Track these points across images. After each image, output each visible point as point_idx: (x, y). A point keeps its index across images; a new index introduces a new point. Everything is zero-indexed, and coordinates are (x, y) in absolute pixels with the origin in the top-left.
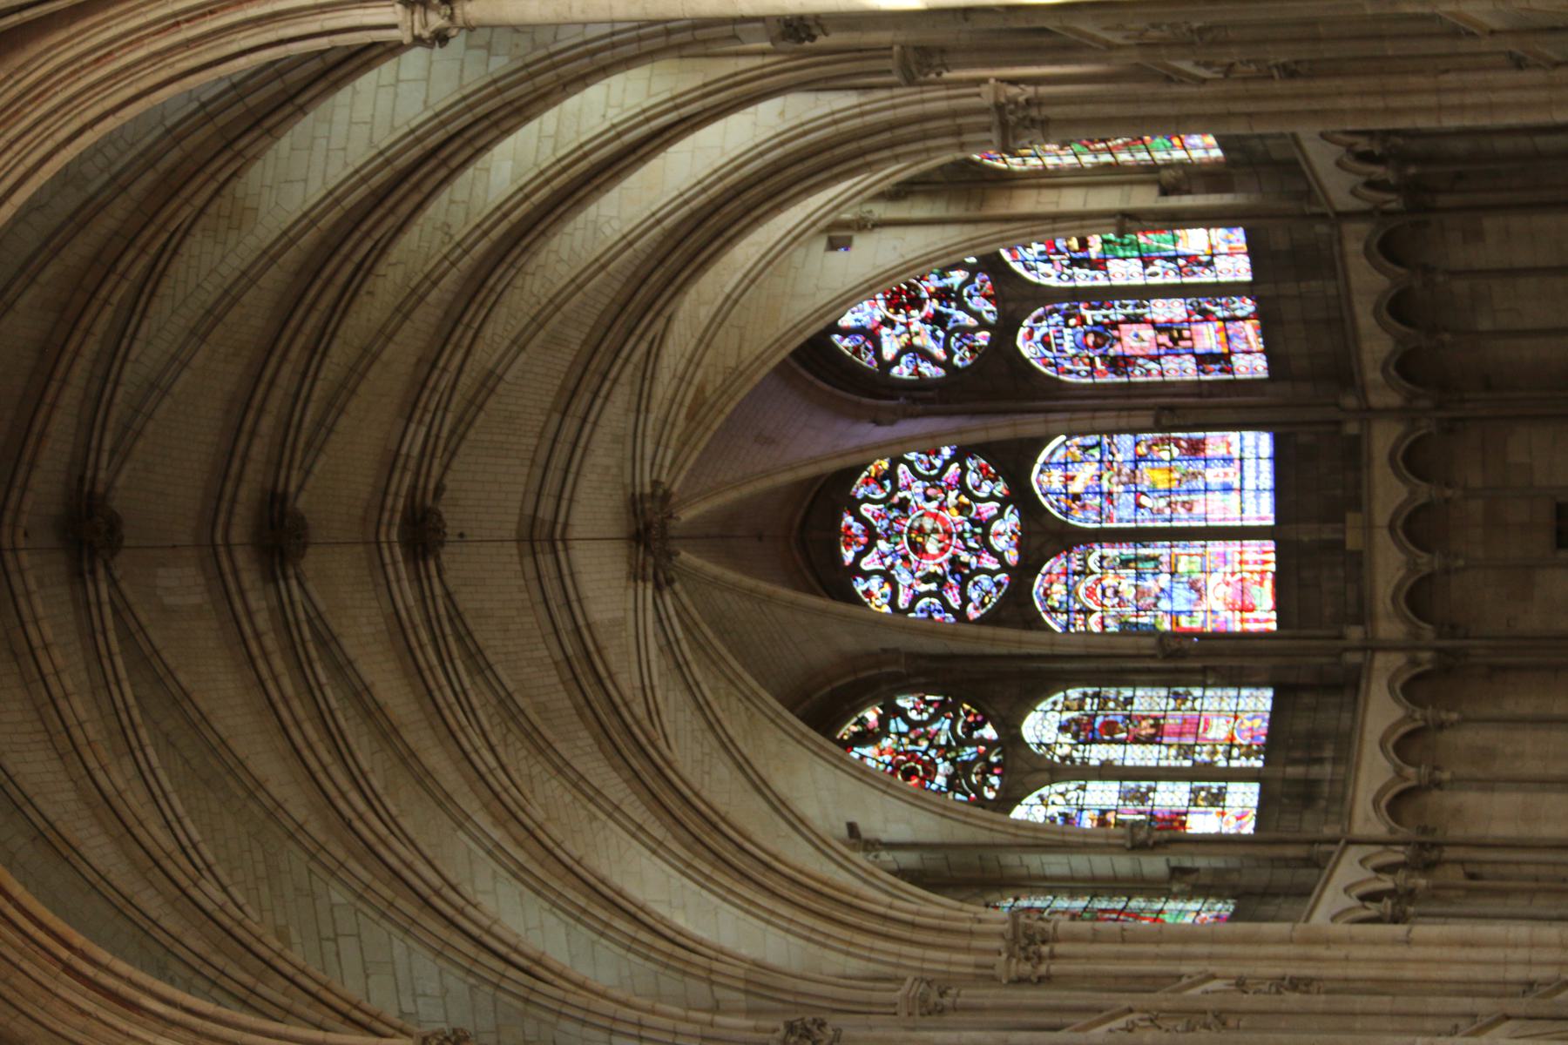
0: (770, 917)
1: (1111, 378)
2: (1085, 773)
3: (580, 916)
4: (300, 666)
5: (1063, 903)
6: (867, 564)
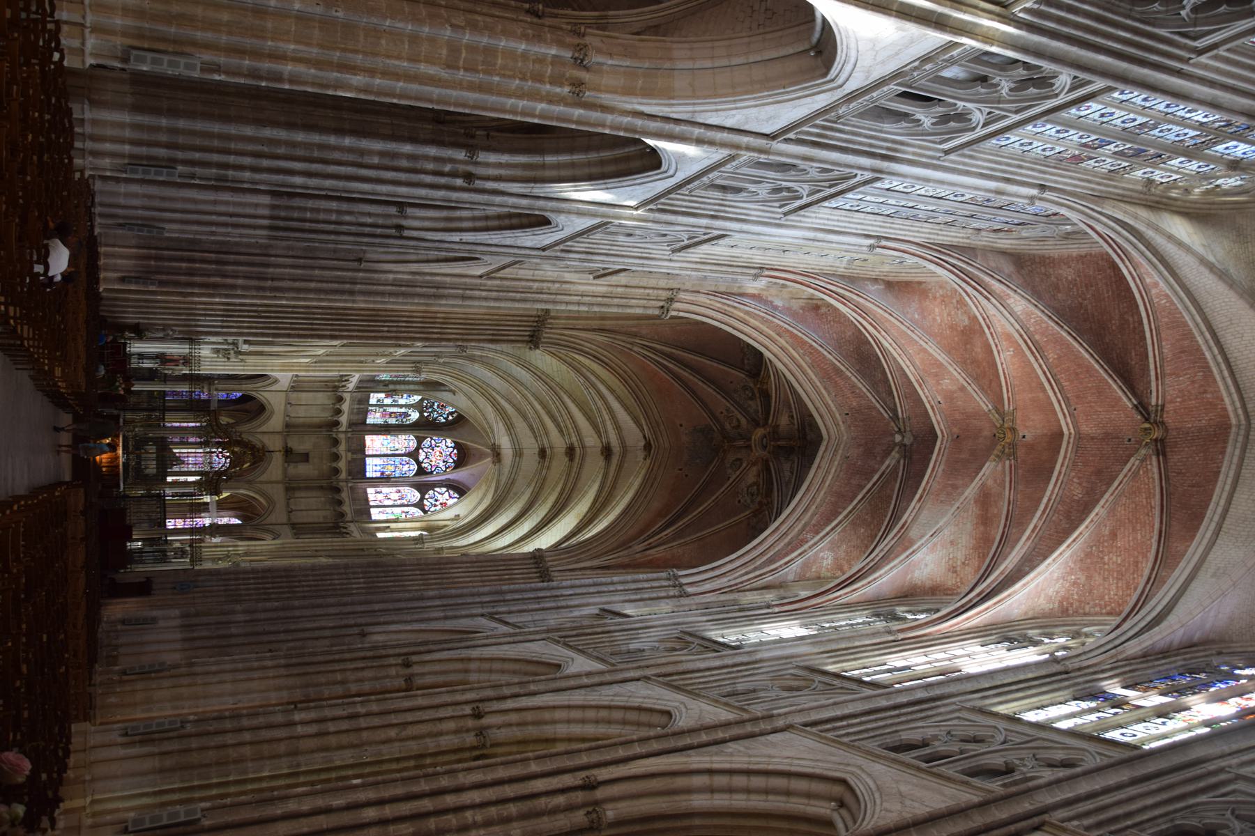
1: (401, 488)
2: (406, 406)
3: (510, 375)
6: (451, 449)
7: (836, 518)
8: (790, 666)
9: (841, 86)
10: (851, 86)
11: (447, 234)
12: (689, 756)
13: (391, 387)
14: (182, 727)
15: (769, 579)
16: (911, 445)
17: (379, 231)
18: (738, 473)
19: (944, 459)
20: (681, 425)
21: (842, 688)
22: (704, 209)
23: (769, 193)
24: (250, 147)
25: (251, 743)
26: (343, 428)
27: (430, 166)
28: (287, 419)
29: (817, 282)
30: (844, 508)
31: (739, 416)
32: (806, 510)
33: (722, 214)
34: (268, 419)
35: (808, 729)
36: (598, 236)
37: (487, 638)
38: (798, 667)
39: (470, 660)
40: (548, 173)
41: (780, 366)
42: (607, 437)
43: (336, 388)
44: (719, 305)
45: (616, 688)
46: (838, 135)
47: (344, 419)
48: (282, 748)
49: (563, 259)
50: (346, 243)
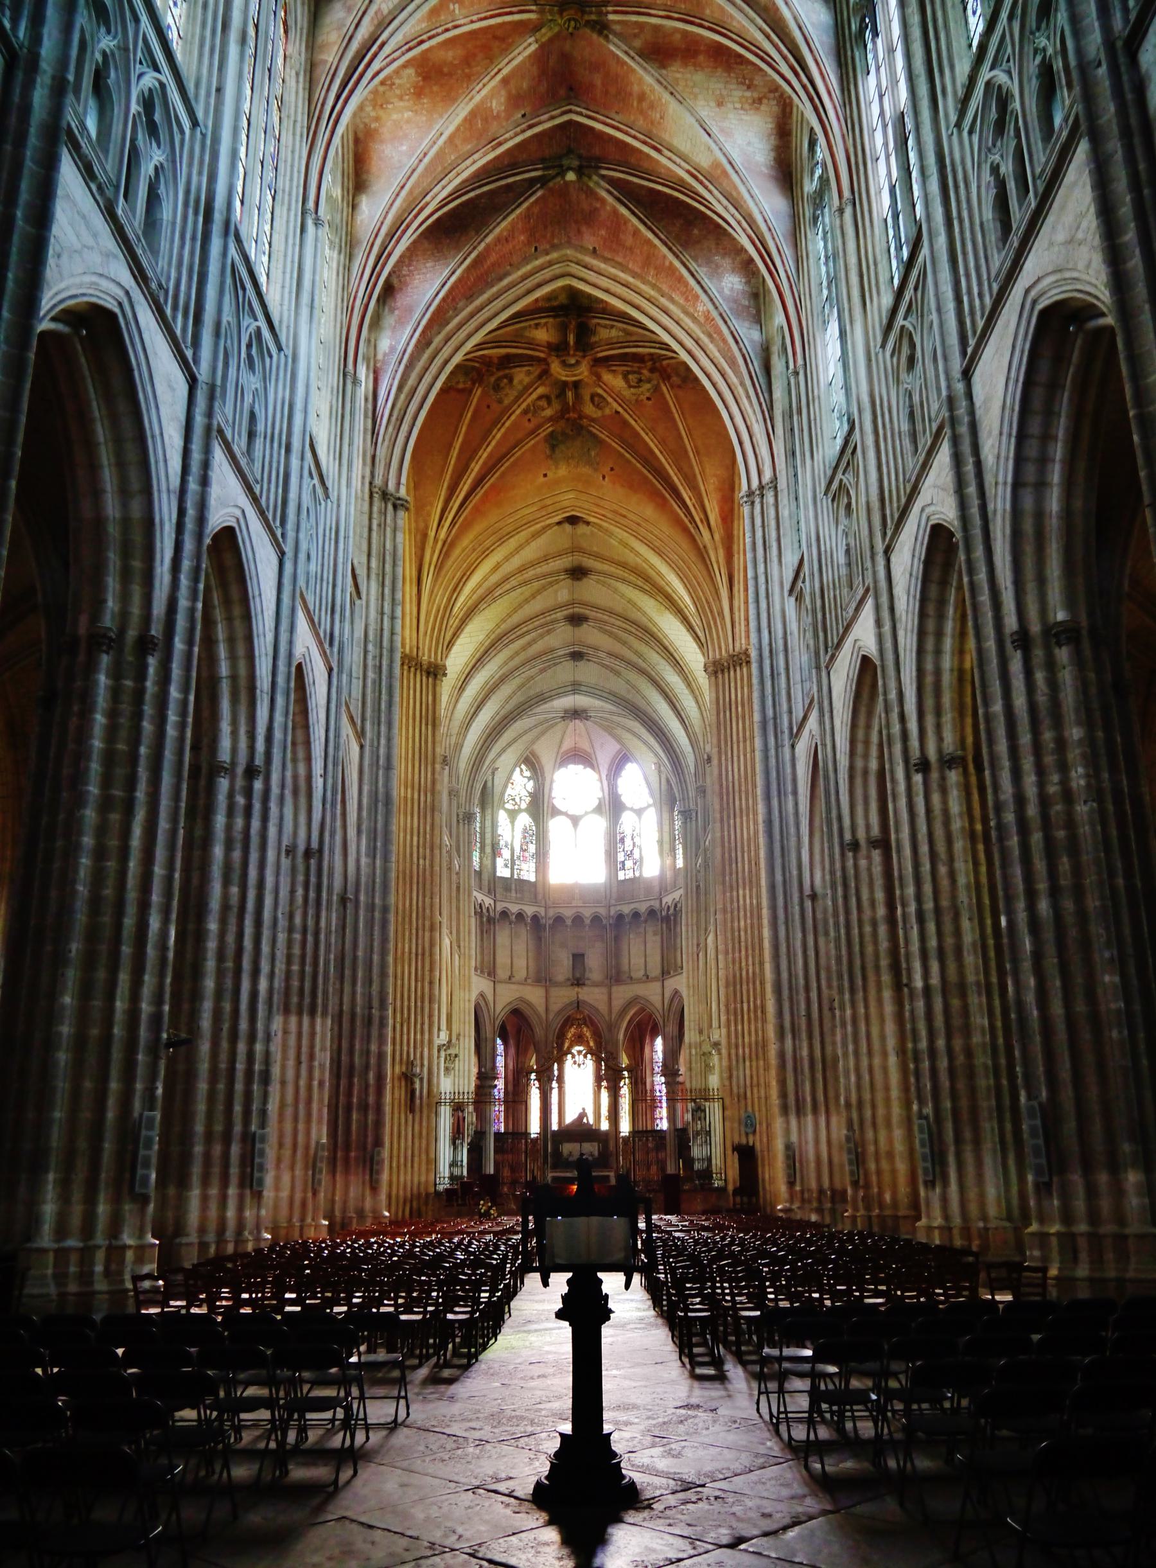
0: (474, 748)
2: (513, 830)
4: (542, 626)
5: (478, 825)
7: (676, 269)
8: (880, 356)
9: (127, 293)
10: (126, 277)
11: (314, 795)
12: (995, 511)
13: (488, 849)
14: (926, 1118)
15: (757, 365)
16: (580, 157)
17: (313, 879)
18: (610, 400)
19: (603, 111)
20: (545, 475)
21: (916, 289)
22: (279, 462)
23: (254, 373)
24: (225, 1045)
25: (949, 1038)
26: (542, 911)
27: (239, 822)
28: (529, 981)
29: (360, 294)
30: (665, 257)
31: (534, 396)
32: (666, 312)
33: (284, 437)
34: (529, 1004)
35: (970, 350)
36: (310, 599)
37: (824, 745)
38: (883, 346)
39: (852, 768)
40: (242, 671)
41: (469, 345)
42: (558, 572)
43: (490, 920)
44: (390, 429)
45: (900, 590)
46: (183, 287)
47: (530, 910)
48: (956, 1002)
49: (341, 644)
50: (330, 919)
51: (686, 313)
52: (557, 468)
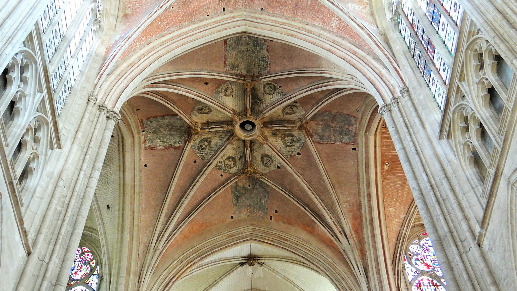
15: (379, 39)
20: (232, 217)
44: (112, 77)
51: (323, 29)
52: (240, 213)
